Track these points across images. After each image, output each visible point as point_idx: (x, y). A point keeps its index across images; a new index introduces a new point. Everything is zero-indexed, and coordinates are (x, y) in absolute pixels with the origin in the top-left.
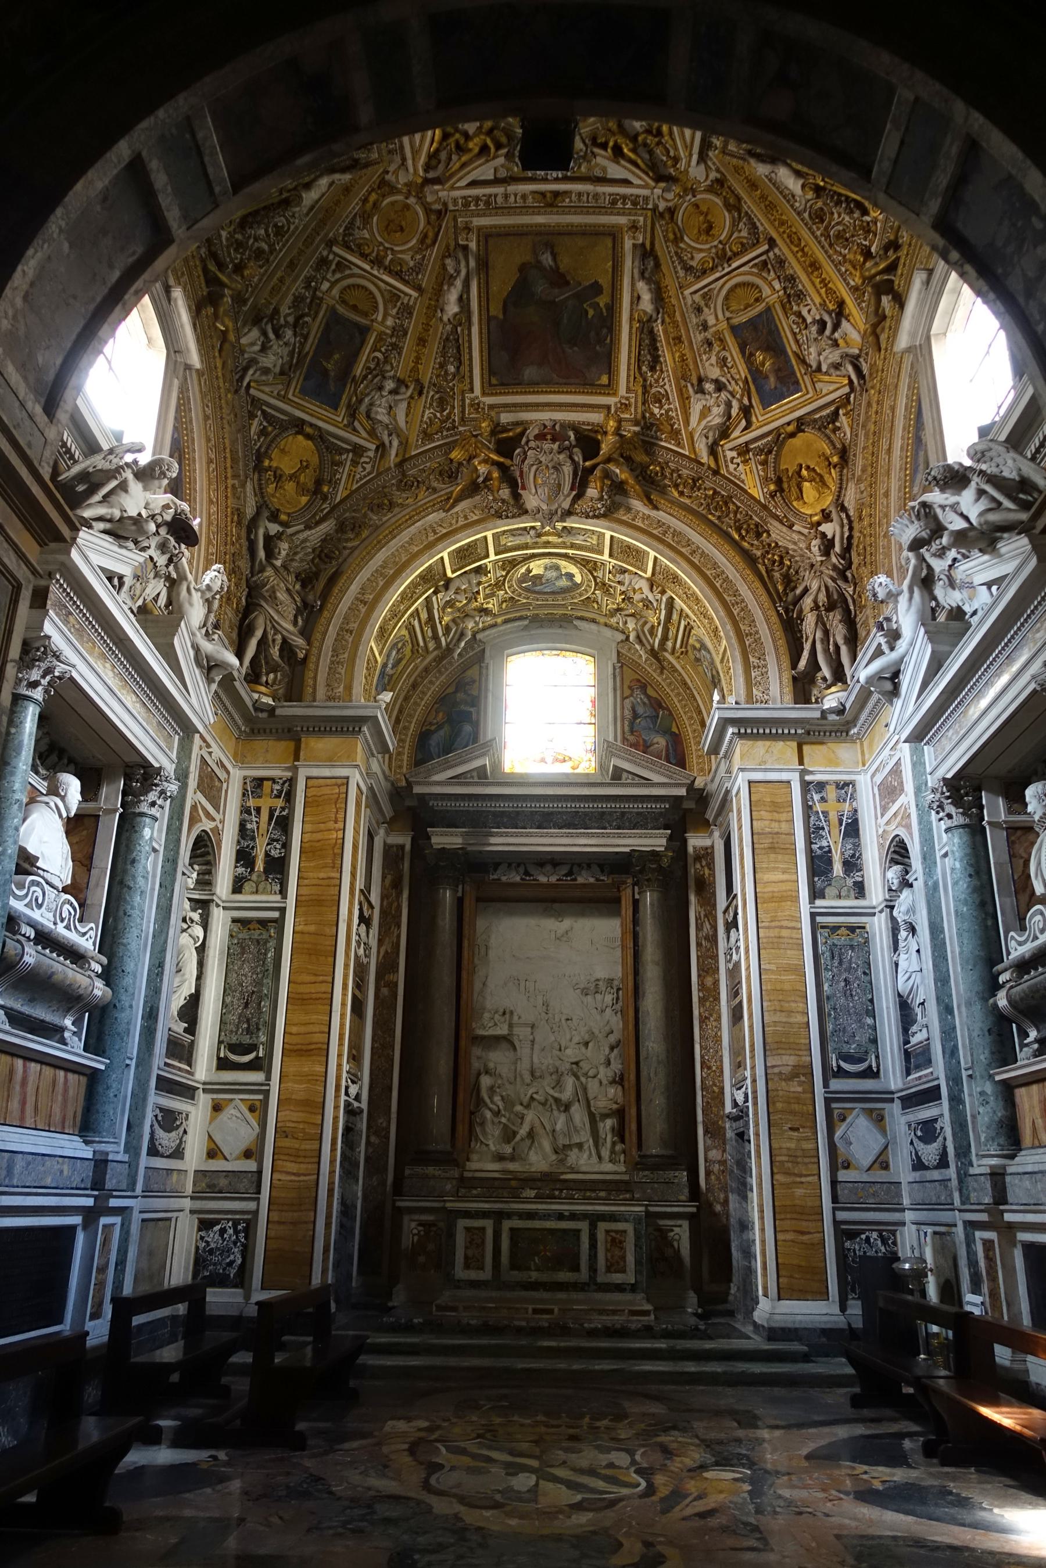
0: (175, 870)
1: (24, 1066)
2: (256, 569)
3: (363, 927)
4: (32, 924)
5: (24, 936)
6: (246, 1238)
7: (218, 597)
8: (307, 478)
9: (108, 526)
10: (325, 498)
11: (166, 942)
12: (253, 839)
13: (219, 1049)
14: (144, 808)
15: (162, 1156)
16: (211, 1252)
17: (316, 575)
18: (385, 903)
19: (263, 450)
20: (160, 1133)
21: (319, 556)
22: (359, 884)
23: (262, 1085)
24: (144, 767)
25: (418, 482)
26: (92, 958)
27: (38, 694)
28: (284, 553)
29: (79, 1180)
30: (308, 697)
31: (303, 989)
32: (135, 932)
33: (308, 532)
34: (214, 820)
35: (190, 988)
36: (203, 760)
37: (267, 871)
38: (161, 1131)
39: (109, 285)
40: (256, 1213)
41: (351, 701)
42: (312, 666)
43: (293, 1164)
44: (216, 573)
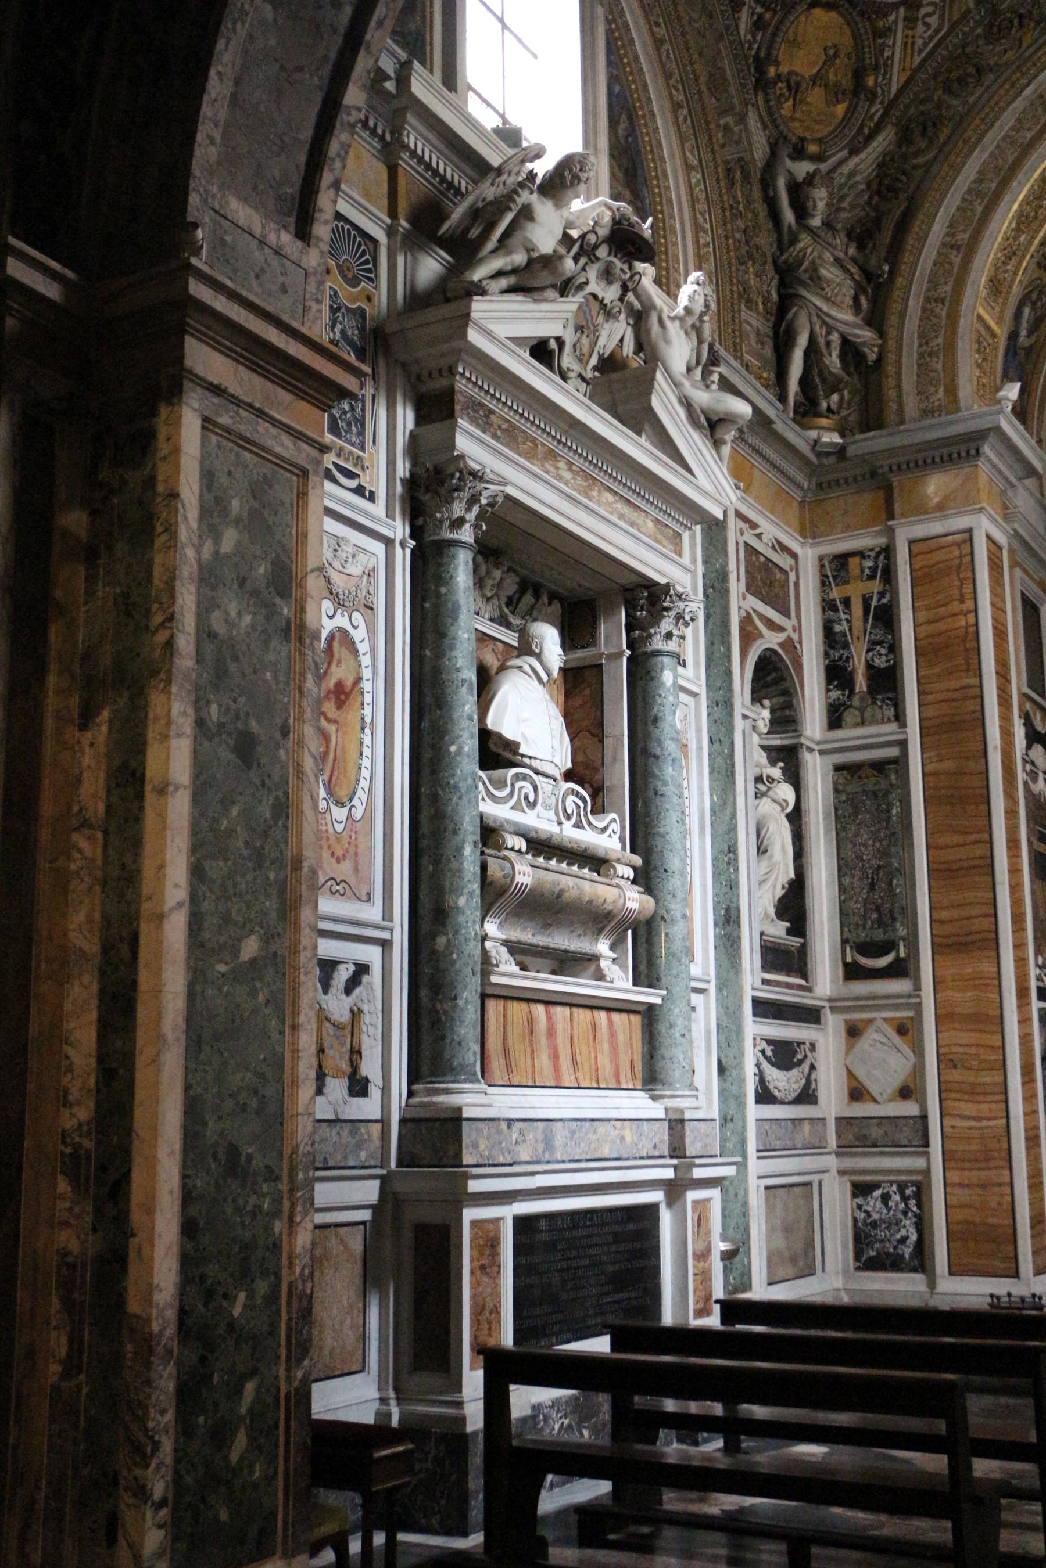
0: (730, 714)
1: (547, 1012)
2: (784, 240)
4: (521, 832)
5: (512, 849)
6: (919, 1205)
7: (706, 318)
8: (840, 75)
9: (512, 280)
10: (872, 96)
11: (734, 816)
12: (846, 646)
13: (844, 952)
14: (658, 643)
15: (782, 1102)
16: (874, 1224)
17: (877, 223)
19: (763, 54)
20: (773, 1074)
21: (878, 193)
23: (910, 996)
24: (647, 587)
25: (1021, 17)
26: (618, 861)
27: (466, 534)
28: (821, 205)
29: (650, 1146)
30: (891, 417)
31: (950, 855)
32: (673, 816)
33: (856, 160)
34: (781, 629)
35: (787, 872)
36: (750, 550)
38: (775, 1070)
39: (342, 30)
40: (927, 1172)
41: (958, 410)
42: (890, 369)
43: (970, 1105)
44: (696, 287)
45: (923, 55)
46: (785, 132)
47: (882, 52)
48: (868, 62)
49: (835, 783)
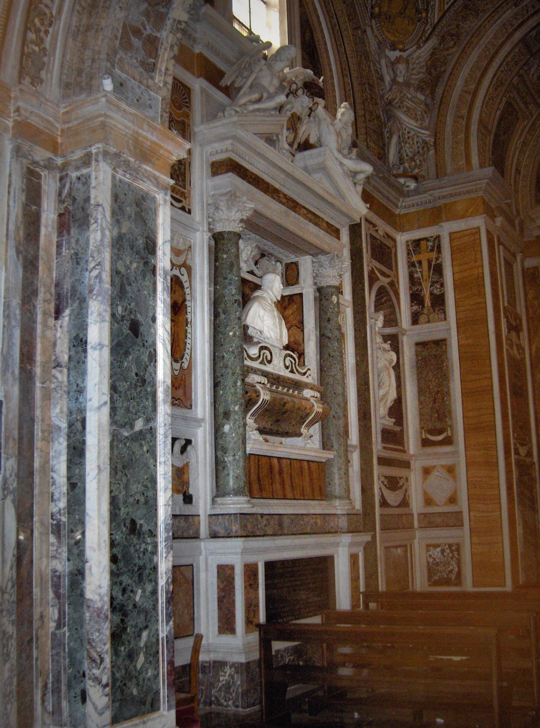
3: (514, 334)
6: (459, 555)
12: (420, 284)
13: (421, 433)
15: (392, 507)
16: (437, 564)
18: (531, 310)
20: (387, 494)
22: (503, 302)
36: (373, 238)
37: (433, 305)
45: (449, 4)
49: (416, 351)
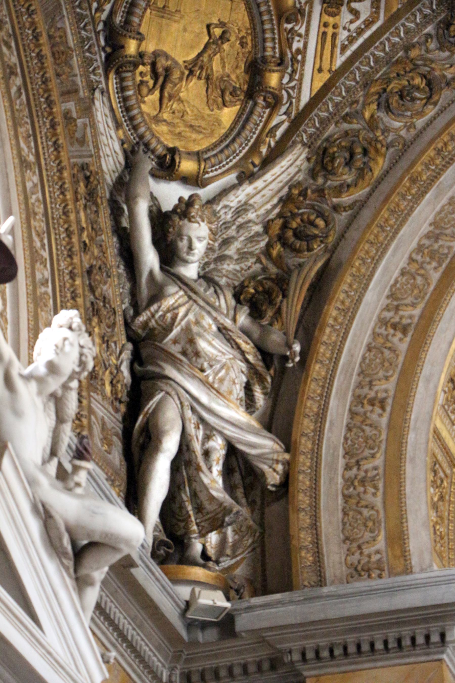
19: (118, 19)
21: (281, 238)
45: (348, 53)
46: (148, 136)
47: (290, 44)
48: (269, 53)
